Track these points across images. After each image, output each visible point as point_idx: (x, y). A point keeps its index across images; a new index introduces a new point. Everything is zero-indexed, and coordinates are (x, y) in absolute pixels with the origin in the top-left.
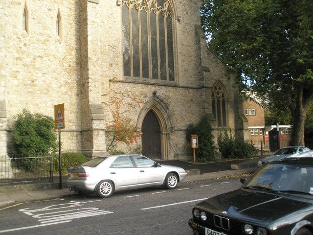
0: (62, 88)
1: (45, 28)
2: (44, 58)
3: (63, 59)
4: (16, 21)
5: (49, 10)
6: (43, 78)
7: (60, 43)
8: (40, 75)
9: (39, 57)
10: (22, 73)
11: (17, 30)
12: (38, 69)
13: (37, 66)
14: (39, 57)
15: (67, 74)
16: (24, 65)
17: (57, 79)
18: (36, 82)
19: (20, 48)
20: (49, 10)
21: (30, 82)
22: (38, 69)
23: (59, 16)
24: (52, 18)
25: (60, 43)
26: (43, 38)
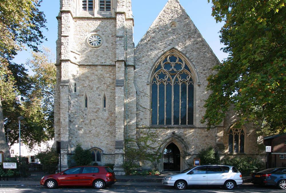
0: (106, 134)
1: (97, 105)
2: (96, 120)
3: (107, 119)
4: (81, 104)
5: (99, 95)
6: (95, 129)
7: (105, 111)
8: (94, 128)
9: (93, 119)
10: (84, 128)
11: (81, 108)
12: (93, 125)
13: (92, 124)
14: (93, 119)
15: (109, 127)
16: (85, 124)
17: (103, 129)
18: (92, 132)
19: (83, 116)
20: (99, 95)
21: (88, 132)
22: (93, 125)
23: (105, 98)
24: (101, 99)
25: (105, 111)
26: (95, 110)
